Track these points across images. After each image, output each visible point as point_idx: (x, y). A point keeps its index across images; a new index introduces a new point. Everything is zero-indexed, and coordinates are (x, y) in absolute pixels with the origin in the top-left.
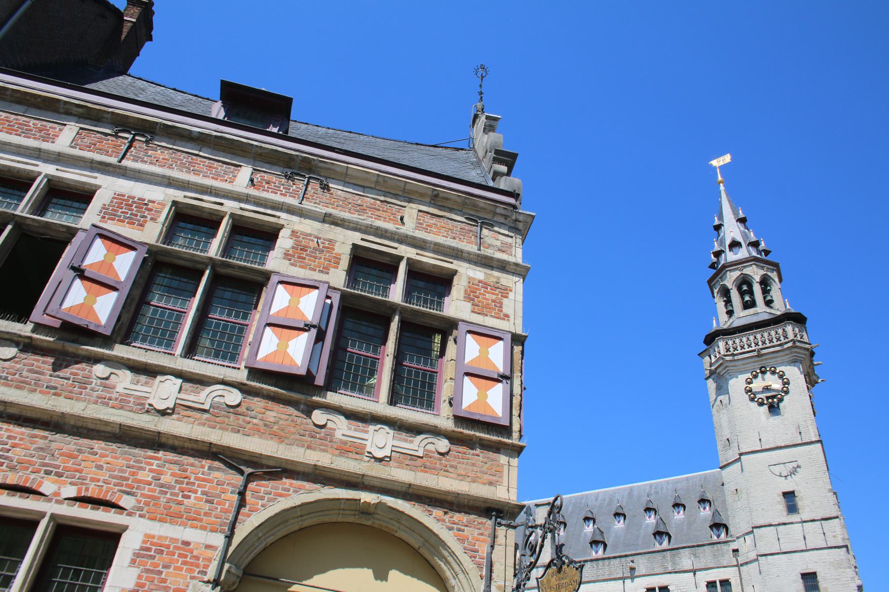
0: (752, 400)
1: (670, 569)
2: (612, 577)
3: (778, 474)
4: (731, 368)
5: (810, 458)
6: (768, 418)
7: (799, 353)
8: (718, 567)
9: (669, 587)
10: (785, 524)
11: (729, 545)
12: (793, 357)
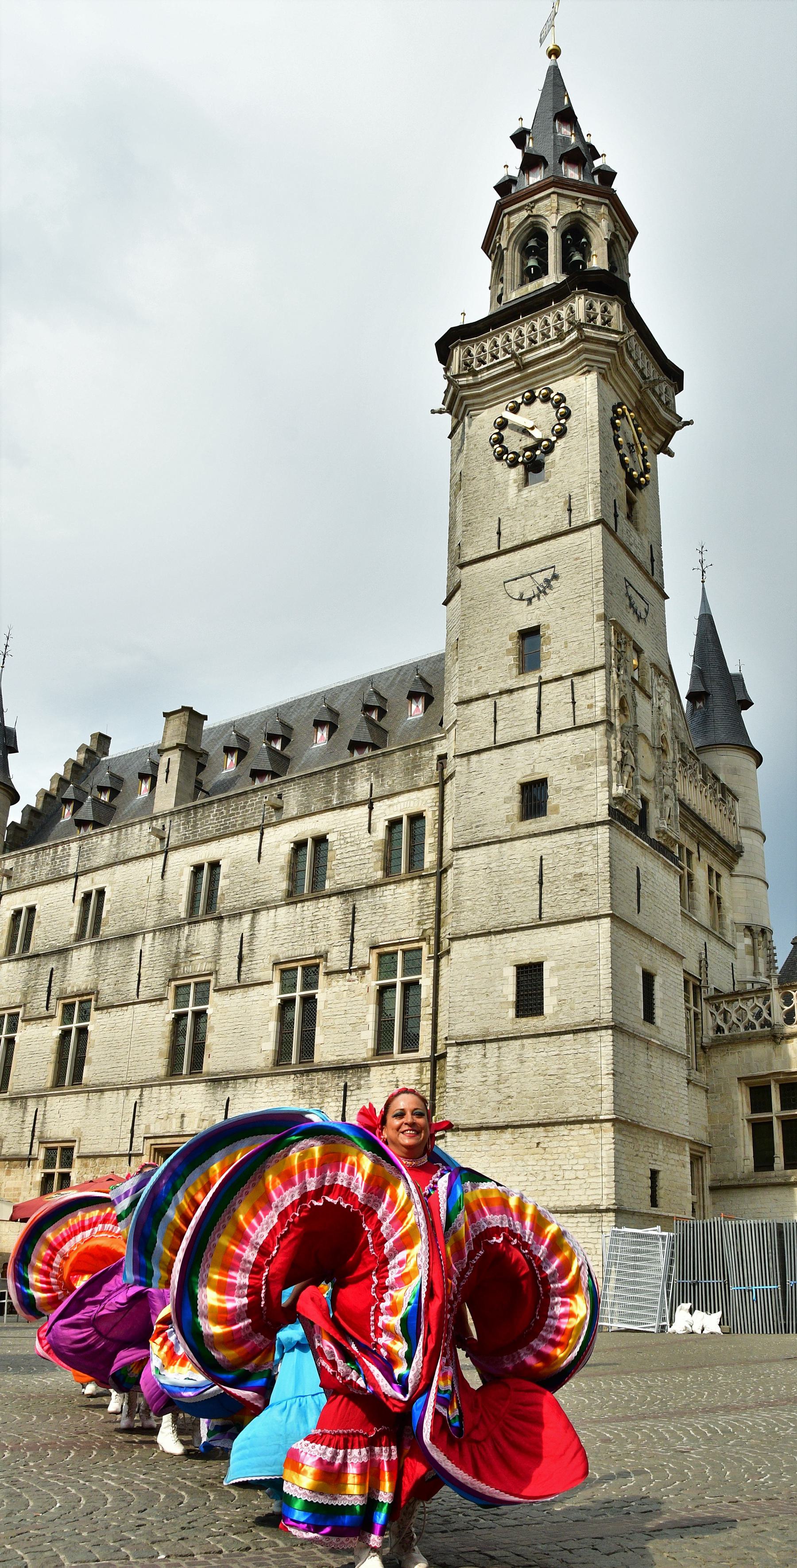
0: (499, 458)
1: (335, 802)
2: (247, 826)
3: (517, 597)
4: (471, 401)
5: (576, 559)
6: (520, 491)
7: (595, 352)
8: (409, 791)
9: (328, 837)
10: (510, 691)
11: (433, 748)
12: (581, 362)
